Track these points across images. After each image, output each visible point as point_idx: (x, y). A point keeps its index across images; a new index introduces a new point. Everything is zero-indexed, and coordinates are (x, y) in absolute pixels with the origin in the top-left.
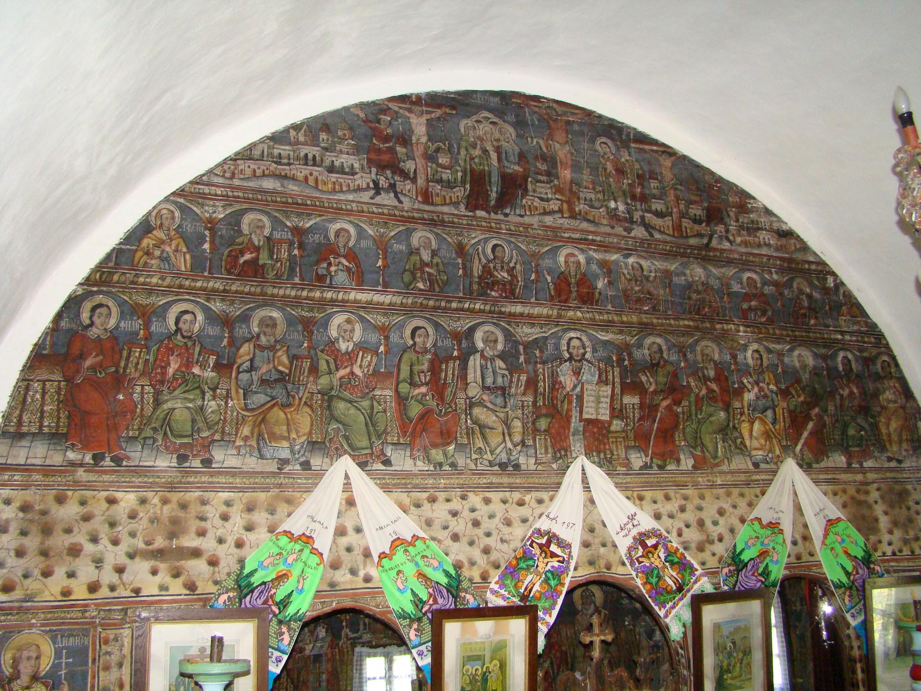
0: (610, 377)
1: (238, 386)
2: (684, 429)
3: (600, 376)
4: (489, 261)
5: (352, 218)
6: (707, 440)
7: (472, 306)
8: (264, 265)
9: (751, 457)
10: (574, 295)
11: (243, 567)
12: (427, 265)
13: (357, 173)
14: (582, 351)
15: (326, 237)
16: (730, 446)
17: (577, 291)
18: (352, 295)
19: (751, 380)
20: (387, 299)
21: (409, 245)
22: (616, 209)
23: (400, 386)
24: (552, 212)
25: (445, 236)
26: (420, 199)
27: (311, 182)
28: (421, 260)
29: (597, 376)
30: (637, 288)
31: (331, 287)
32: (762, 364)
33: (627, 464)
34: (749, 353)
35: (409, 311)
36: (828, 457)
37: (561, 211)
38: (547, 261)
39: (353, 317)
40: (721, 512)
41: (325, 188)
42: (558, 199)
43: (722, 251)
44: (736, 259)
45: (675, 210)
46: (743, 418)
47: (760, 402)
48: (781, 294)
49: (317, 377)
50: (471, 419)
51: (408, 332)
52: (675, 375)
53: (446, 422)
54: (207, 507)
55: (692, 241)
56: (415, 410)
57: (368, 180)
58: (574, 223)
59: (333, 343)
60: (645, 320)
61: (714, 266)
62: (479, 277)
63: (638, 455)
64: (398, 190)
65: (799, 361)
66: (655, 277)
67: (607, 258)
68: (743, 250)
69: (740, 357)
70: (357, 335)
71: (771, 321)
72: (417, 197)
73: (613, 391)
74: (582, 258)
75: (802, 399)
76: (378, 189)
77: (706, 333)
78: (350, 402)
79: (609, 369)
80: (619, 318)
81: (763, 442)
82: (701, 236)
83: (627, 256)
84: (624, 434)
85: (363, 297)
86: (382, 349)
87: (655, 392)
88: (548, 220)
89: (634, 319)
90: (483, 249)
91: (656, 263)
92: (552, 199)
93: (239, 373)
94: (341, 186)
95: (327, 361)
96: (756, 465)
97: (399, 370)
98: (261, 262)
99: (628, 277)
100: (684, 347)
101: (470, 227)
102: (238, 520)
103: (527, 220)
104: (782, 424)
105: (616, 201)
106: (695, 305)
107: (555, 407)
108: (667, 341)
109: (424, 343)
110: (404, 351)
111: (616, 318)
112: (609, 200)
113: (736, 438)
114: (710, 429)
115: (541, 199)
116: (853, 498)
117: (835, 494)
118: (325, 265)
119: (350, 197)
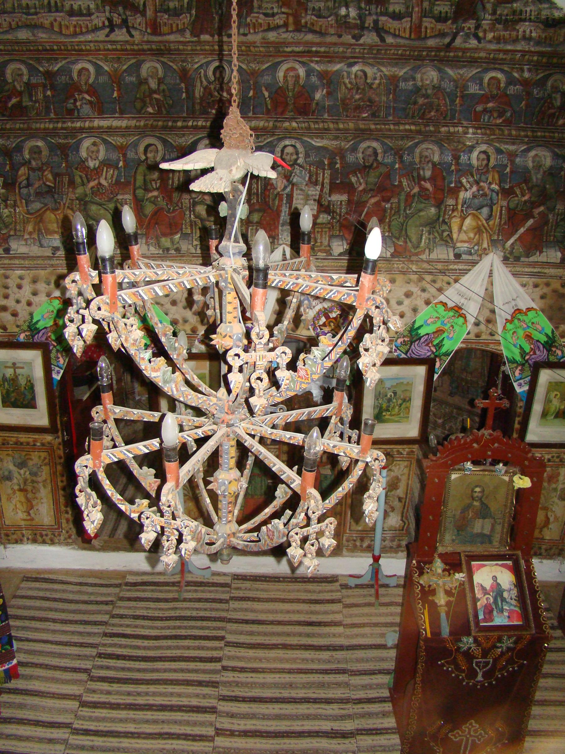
0: (320, 179)
1: (21, 198)
2: (390, 221)
3: (310, 178)
4: (210, 83)
5: (90, 58)
6: (412, 232)
7: (195, 123)
8: (26, 107)
9: (454, 248)
10: (291, 107)
11: (32, 318)
12: (155, 92)
13: (93, 14)
14: (295, 157)
15: (71, 78)
16: (435, 238)
17: (294, 103)
18: (96, 123)
19: (471, 180)
20: (124, 123)
21: (138, 76)
22: (347, 16)
23: (137, 191)
24: (277, 27)
25: (171, 64)
26: (149, 30)
27: (56, 29)
28: (149, 88)
29: (307, 179)
30: (357, 97)
31: (79, 118)
32: (487, 165)
33: (329, 252)
34: (475, 154)
35: (143, 132)
36: (541, 252)
37: (286, 25)
38: (266, 77)
39: (98, 140)
40: (408, 295)
41: (68, 33)
42: (284, 13)
43: (465, 50)
44: (481, 58)
45: (416, 9)
46: (455, 214)
47: (476, 201)
48: (528, 94)
49: (75, 188)
50: (194, 214)
51: (141, 149)
52: (388, 176)
53: (174, 217)
54: (9, 280)
55: (431, 43)
56: (149, 209)
57: (103, 19)
58: (299, 36)
59: (84, 162)
60: (362, 126)
61: (452, 67)
62: (201, 98)
63: (340, 243)
64: (130, 25)
65: (533, 162)
66: (380, 84)
67: (329, 69)
68: (493, 47)
69: (464, 158)
70: (102, 155)
71: (508, 123)
72: (146, 29)
73: (322, 190)
74: (302, 72)
75: (526, 198)
76: (112, 27)
77: (426, 137)
78: (100, 205)
79: (320, 172)
80: (336, 126)
81: (472, 235)
82: (442, 35)
83: (351, 65)
84: (329, 226)
85: (105, 123)
86: (121, 164)
87: (364, 190)
88: (272, 36)
89: (351, 125)
90: (205, 72)
91: (384, 69)
92: (277, 13)
93: (20, 188)
94: (81, 27)
95: (81, 177)
96: (458, 256)
97: (135, 180)
98: (24, 104)
99: (349, 86)
100: (401, 150)
101: (194, 53)
102: (27, 289)
103: (250, 38)
104: (497, 220)
105: (347, 7)
106: (420, 110)
107: (267, 203)
108: (383, 144)
109: (155, 157)
110: (139, 165)
111: (331, 126)
112: (340, 7)
113: (443, 231)
114: (418, 223)
115: (266, 15)
116: (555, 291)
117: (536, 286)
118: (72, 101)
119: (89, 37)
